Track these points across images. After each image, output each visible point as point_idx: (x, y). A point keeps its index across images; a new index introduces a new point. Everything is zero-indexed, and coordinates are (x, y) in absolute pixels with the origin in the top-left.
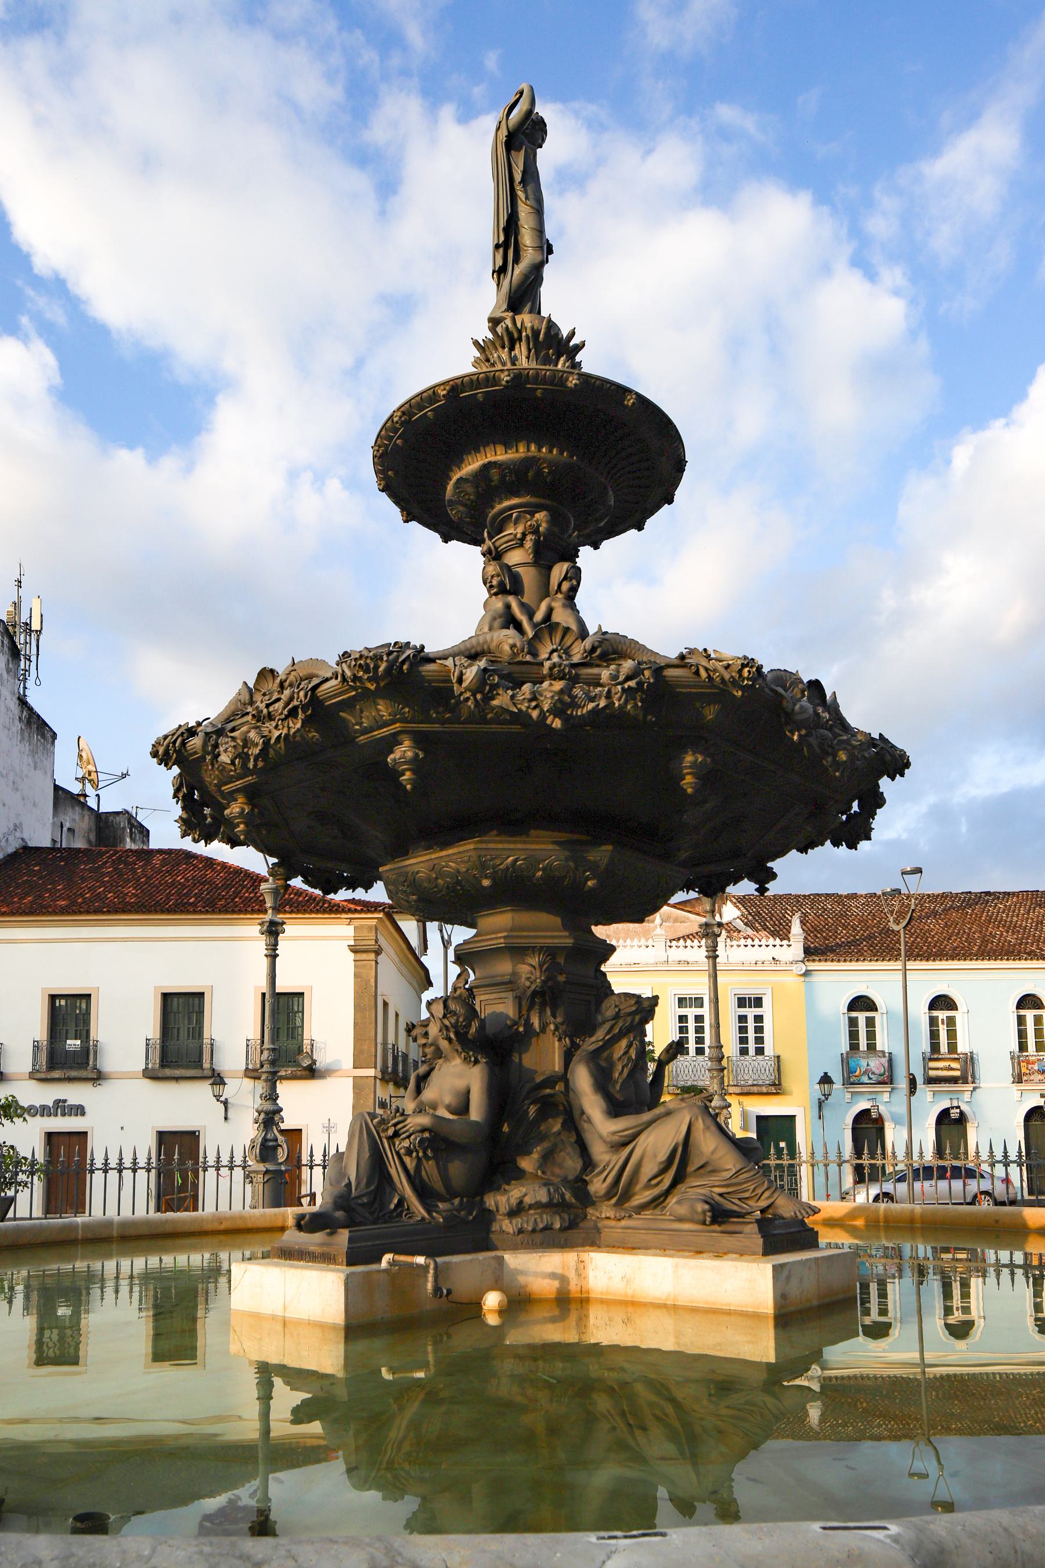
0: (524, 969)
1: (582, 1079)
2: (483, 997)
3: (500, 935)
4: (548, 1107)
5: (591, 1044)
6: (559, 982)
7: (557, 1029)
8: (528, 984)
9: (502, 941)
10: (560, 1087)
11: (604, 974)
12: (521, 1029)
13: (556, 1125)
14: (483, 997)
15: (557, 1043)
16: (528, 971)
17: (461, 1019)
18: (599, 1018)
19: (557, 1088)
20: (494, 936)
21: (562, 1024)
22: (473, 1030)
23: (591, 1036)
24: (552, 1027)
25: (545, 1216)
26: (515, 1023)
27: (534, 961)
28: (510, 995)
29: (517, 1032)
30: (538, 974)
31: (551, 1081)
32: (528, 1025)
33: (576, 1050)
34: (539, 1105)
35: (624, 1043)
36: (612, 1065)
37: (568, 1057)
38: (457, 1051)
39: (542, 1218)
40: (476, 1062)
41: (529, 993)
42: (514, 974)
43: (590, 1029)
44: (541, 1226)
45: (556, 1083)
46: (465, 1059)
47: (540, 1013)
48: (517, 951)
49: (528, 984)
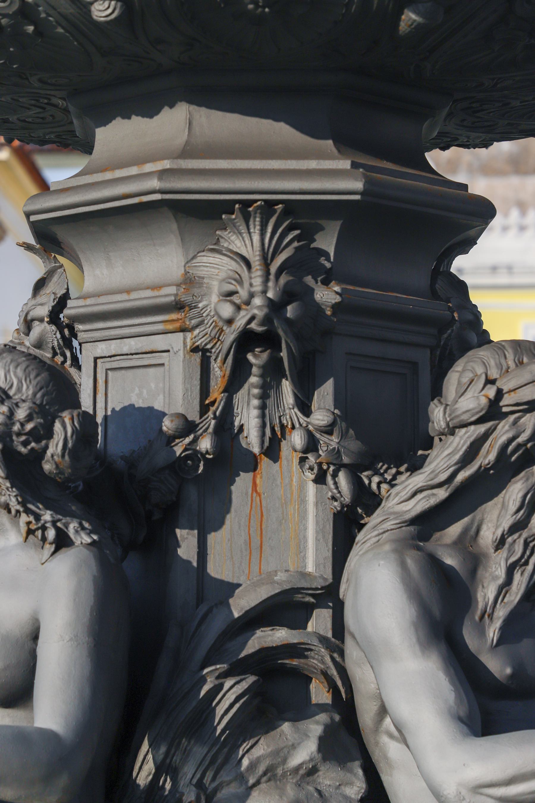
0: (216, 268)
1: (380, 596)
2: (101, 349)
3: (149, 168)
4: (279, 687)
5: (406, 496)
6: (318, 308)
7: (312, 445)
8: (227, 310)
9: (154, 183)
10: (320, 622)
11: (461, 288)
12: (205, 444)
13: (301, 742)
14: (101, 349)
15: (311, 488)
16: (230, 276)
17: (21, 414)
18: (438, 416)
19: (311, 627)
20: (134, 171)
21: (328, 430)
22: (55, 447)
23: (415, 466)
24: (297, 439)
26: (189, 427)
27: (246, 241)
28: (176, 342)
29: (194, 455)
30: (258, 283)
31: (286, 608)
32: (226, 429)
33: (370, 511)
34: (251, 679)
35: (515, 492)
36: (475, 561)
37: (346, 528)
38: (7, 508)
40: (62, 542)
41: (230, 336)
42: (190, 281)
43: (409, 447)
45: (307, 610)
46: (30, 532)
47: (264, 397)
48: (200, 214)
49: (227, 310)
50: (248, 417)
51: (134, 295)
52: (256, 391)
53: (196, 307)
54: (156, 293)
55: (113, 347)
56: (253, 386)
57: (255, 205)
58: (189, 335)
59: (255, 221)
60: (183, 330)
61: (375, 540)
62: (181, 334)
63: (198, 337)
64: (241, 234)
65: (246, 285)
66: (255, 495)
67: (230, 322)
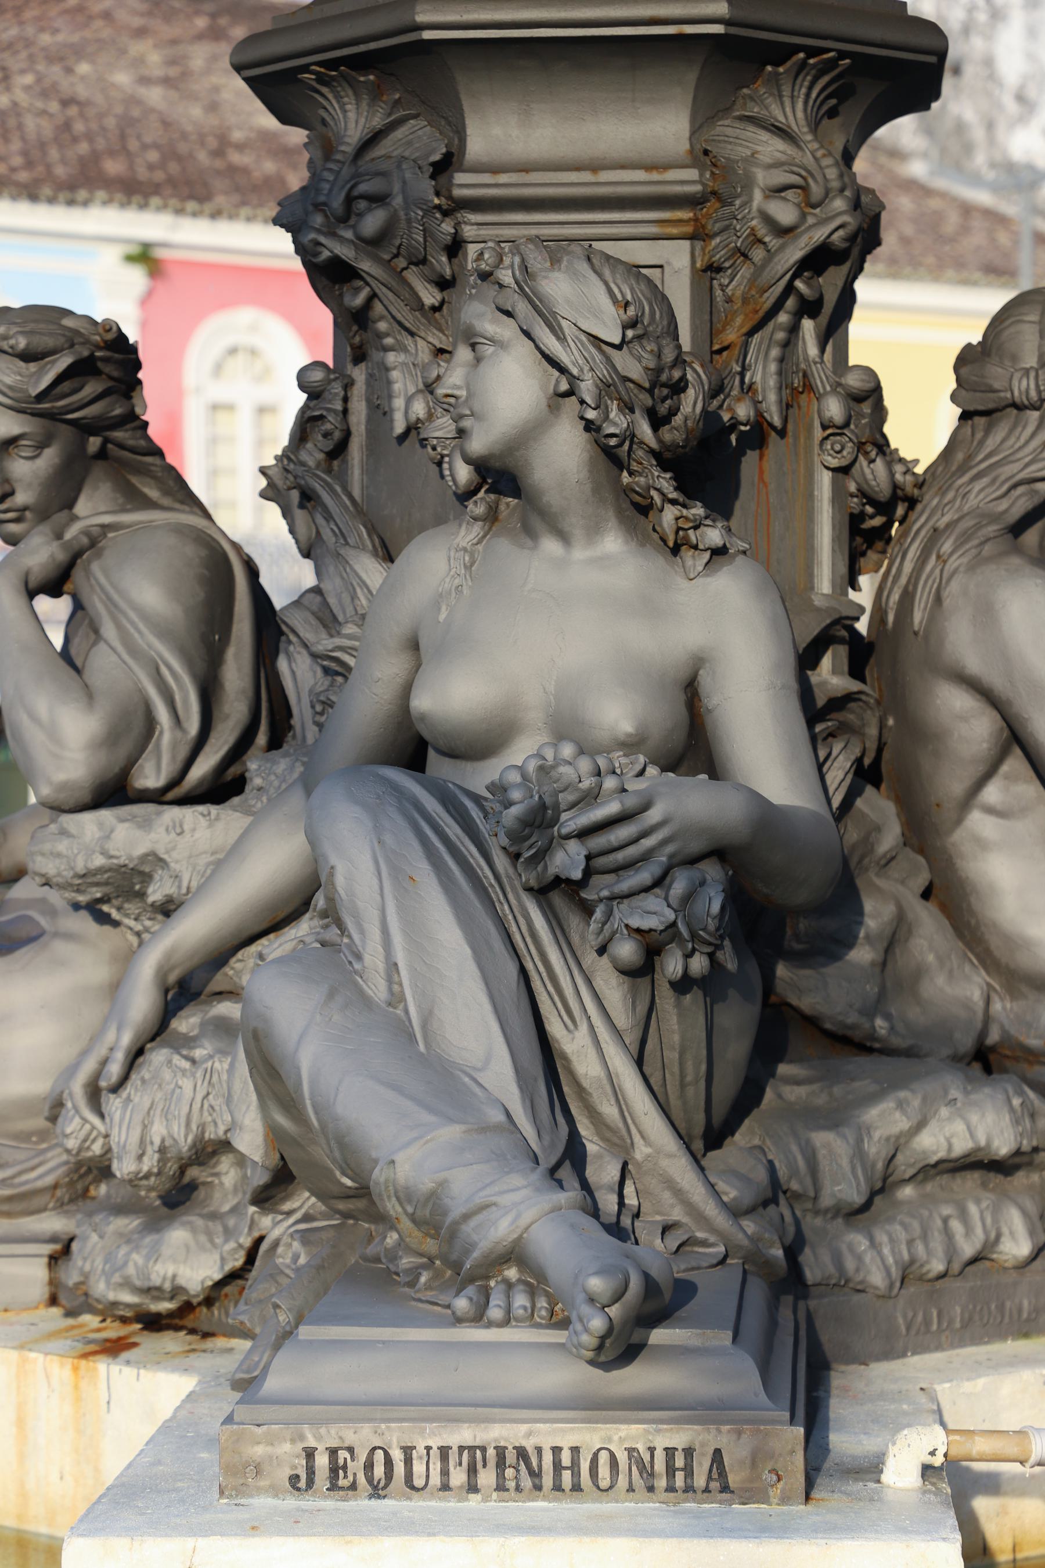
15: (825, 480)
25: (973, 1209)
39: (963, 1216)
41: (795, 253)
44: (968, 1250)
49: (785, 213)
50: (764, 373)
51: (605, 176)
52: (781, 335)
53: (731, 204)
54: (655, 176)
56: (780, 327)
57: (825, 56)
58: (699, 245)
59: (804, 80)
60: (692, 237)
61: (974, 552)
62: (686, 244)
63: (718, 247)
64: (781, 96)
65: (819, 178)
66: (761, 485)
67: (784, 232)
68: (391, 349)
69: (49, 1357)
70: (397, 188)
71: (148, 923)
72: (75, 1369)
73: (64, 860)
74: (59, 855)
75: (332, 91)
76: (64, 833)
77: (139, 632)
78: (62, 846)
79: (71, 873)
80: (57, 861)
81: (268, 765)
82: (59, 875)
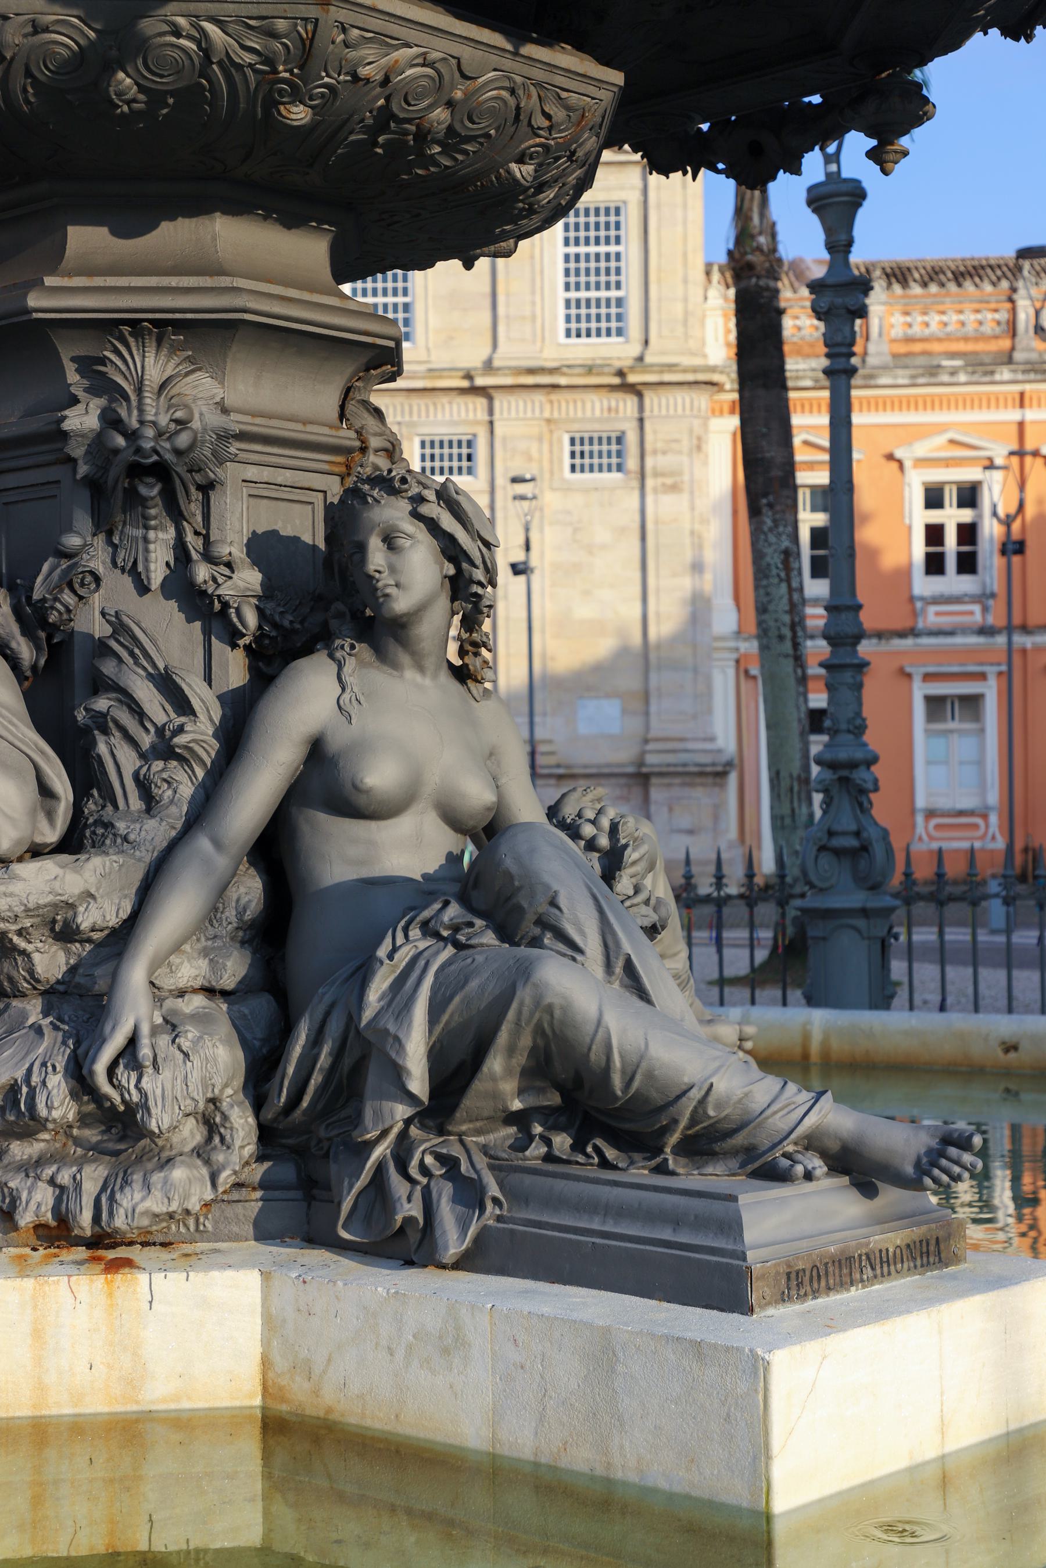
51: (310, 428)
55: (265, 473)
68: (155, 528)
69: (73, 1279)
70: (197, 416)
71: (40, 945)
72: (108, 1283)
73: (16, 898)
74: (11, 895)
75: (137, 342)
76: (15, 877)
77: (13, 724)
78: (17, 887)
79: (23, 908)
80: (9, 899)
81: (138, 826)
82: (10, 909)
